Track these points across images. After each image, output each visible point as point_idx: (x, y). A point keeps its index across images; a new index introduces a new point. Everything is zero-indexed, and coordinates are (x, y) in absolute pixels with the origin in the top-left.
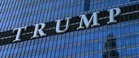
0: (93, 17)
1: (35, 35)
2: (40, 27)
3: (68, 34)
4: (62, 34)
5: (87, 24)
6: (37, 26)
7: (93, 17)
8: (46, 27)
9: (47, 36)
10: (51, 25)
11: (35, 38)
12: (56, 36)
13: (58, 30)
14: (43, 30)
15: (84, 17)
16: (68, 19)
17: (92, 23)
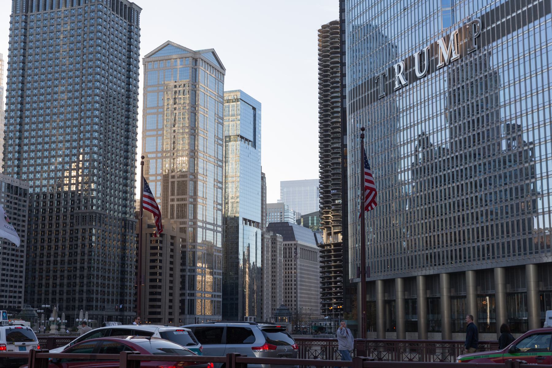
0: (447, 48)
1: (397, 86)
2: (399, 67)
3: (430, 76)
4: (425, 76)
5: (446, 58)
6: (396, 67)
7: (447, 48)
8: (406, 69)
9: (410, 83)
10: (410, 62)
11: (398, 89)
12: (418, 82)
13: (418, 75)
14: (403, 74)
15: (441, 42)
16: (425, 50)
17: (451, 55)
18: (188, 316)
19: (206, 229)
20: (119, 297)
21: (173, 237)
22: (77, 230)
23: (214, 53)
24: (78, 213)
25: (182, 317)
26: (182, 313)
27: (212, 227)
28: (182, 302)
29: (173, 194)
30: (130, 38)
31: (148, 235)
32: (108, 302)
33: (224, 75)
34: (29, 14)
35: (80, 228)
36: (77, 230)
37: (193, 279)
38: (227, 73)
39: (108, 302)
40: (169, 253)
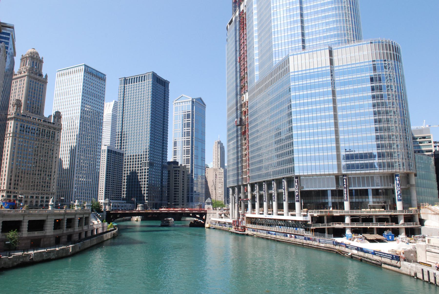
18: (190, 203)
19: (198, 168)
20: (160, 195)
21: (183, 172)
22: (143, 169)
23: (201, 99)
24: (143, 163)
25: (188, 203)
26: (188, 201)
27: (200, 167)
28: (188, 197)
29: (184, 154)
30: (165, 93)
31: (173, 171)
32: (156, 198)
33: (205, 107)
34: (126, 85)
35: (144, 168)
36: (143, 169)
37: (192, 188)
38: (207, 106)
39: (156, 198)
40: (182, 178)
